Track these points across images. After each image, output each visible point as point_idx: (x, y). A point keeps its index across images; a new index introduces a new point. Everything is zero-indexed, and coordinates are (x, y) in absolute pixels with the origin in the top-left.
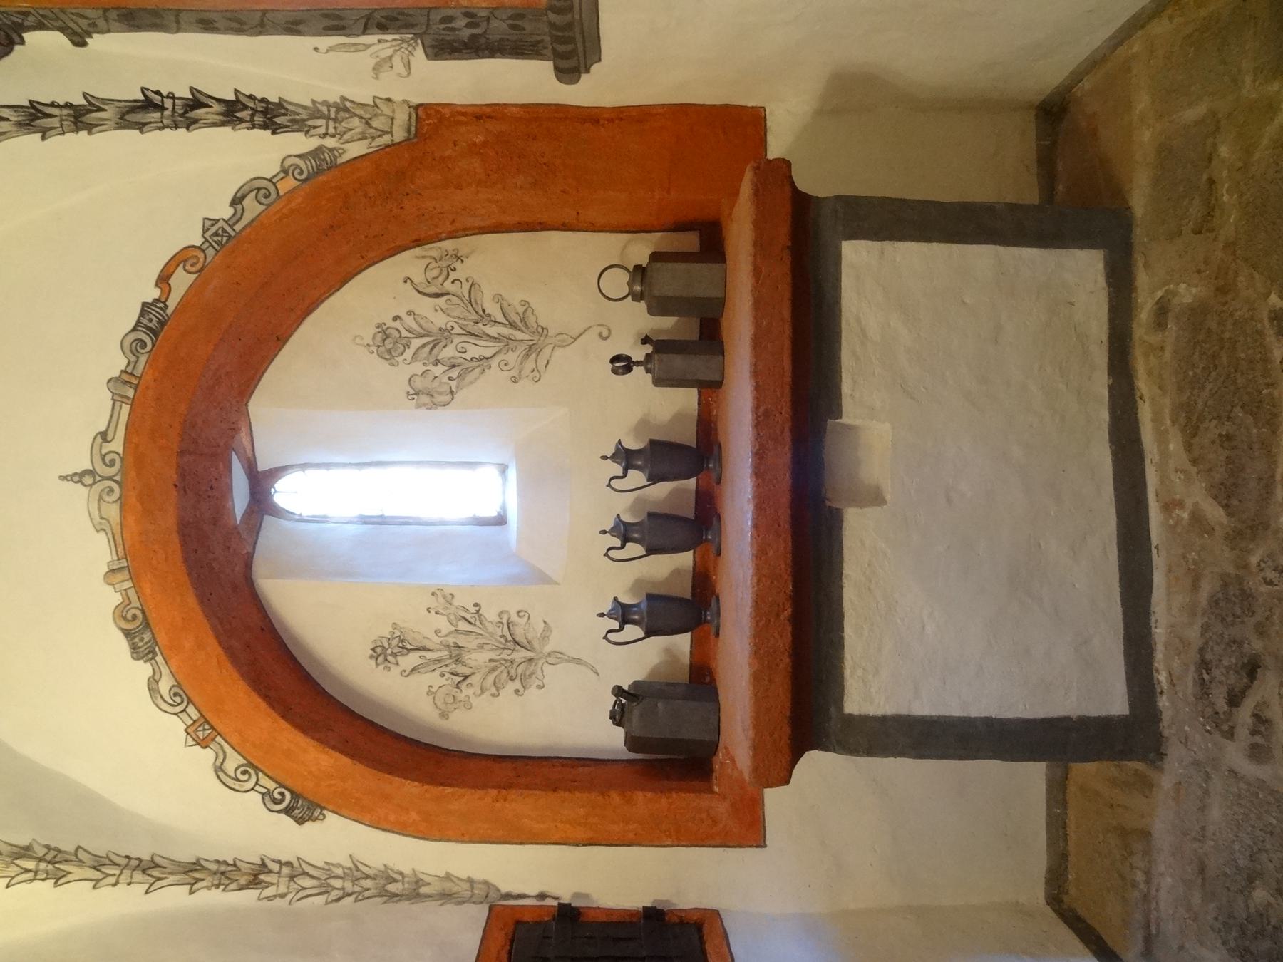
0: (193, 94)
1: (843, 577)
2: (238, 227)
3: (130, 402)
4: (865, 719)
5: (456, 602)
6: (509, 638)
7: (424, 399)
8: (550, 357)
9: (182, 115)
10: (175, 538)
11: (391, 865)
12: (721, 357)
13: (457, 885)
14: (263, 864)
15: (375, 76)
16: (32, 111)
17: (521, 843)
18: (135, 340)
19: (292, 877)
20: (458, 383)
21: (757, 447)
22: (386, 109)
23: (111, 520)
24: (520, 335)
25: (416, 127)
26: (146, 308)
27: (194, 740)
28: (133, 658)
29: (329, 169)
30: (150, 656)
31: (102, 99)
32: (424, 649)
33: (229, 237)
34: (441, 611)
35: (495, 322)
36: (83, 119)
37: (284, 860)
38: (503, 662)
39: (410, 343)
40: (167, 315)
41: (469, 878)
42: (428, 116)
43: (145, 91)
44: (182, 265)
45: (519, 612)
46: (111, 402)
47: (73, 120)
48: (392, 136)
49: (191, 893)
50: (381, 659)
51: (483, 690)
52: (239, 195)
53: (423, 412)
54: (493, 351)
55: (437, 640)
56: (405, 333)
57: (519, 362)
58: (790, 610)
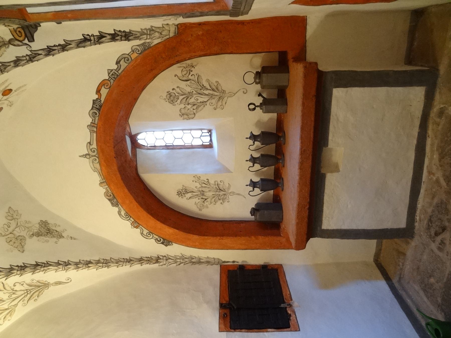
0: (100, 34)
1: (325, 193)
2: (120, 72)
3: (96, 132)
4: (328, 230)
5: (201, 179)
6: (218, 188)
7: (185, 116)
8: (227, 101)
9: (97, 41)
10: (118, 173)
11: (192, 255)
12: (286, 106)
14: (158, 257)
16: (49, 49)
17: (227, 249)
18: (93, 113)
19: (167, 260)
20: (196, 111)
21: (301, 161)
22: (167, 28)
23: (97, 168)
24: (216, 93)
25: (178, 32)
26: (94, 102)
27: (134, 227)
28: (112, 206)
29: (148, 48)
30: (117, 205)
31: (70, 41)
32: (193, 192)
33: (117, 75)
34: (197, 181)
35: (207, 89)
36: (65, 49)
37: (163, 255)
38: (217, 195)
39: (179, 97)
40: (101, 103)
41: (214, 258)
42: (181, 26)
43: (84, 35)
44: (103, 86)
45: (220, 181)
46: (90, 133)
47: (62, 50)
48: (169, 36)
49: (141, 265)
50: (180, 195)
51: (211, 203)
52: (118, 60)
53: (185, 121)
54: (208, 99)
55: (197, 189)
56: (177, 94)
57: (216, 102)
58: (308, 206)
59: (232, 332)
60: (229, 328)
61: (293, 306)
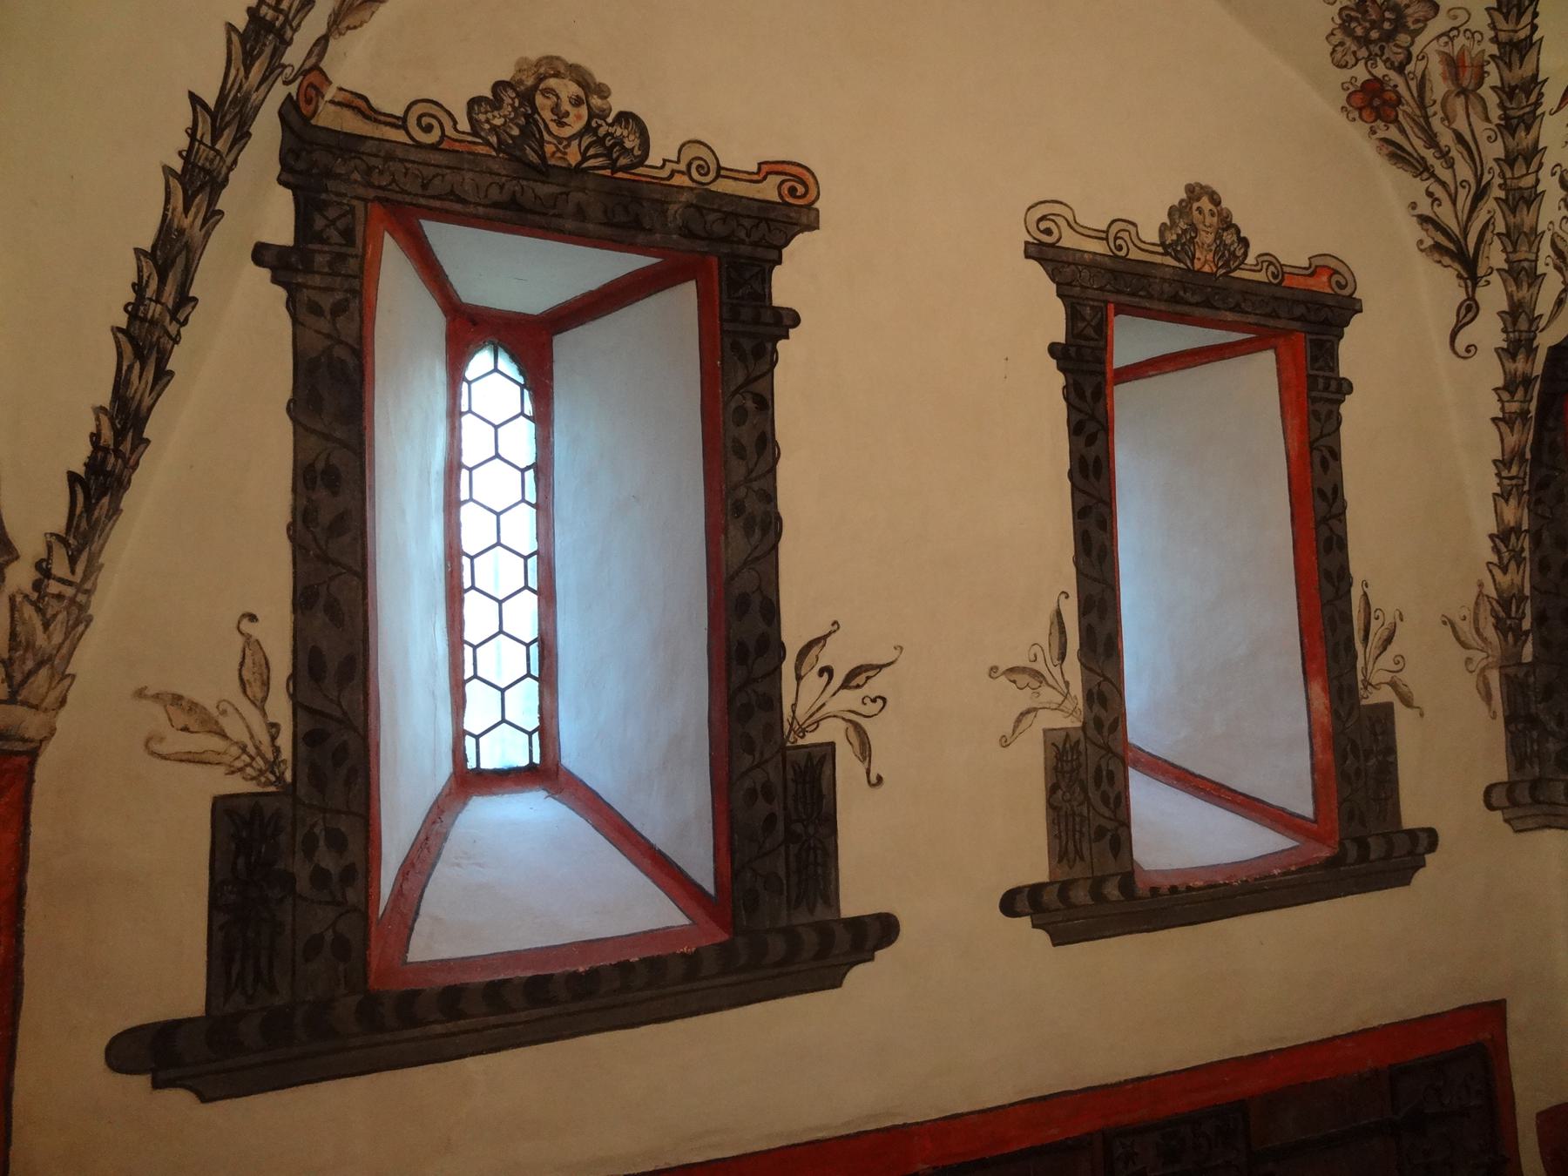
15: (150, 692)
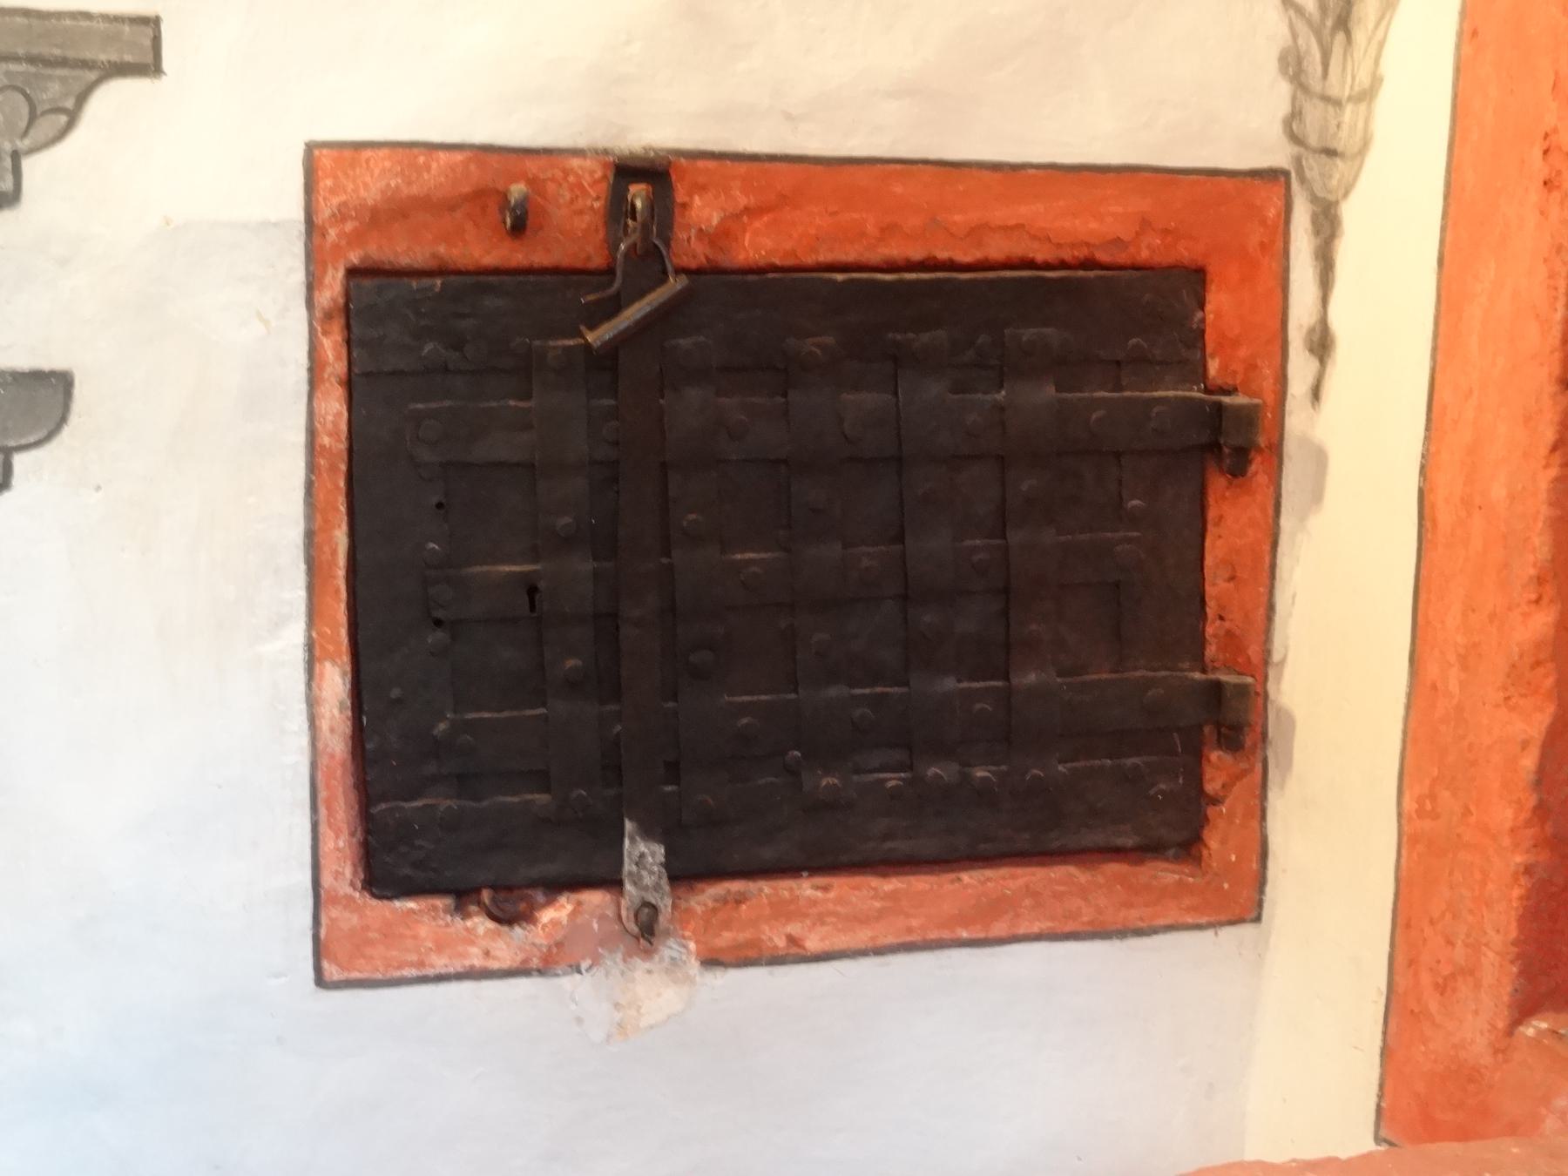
13: (1369, 41)
17: (1441, 261)
59: (311, 287)
60: (354, 258)
61: (640, 965)
